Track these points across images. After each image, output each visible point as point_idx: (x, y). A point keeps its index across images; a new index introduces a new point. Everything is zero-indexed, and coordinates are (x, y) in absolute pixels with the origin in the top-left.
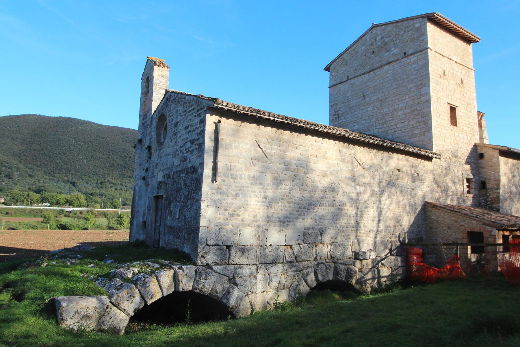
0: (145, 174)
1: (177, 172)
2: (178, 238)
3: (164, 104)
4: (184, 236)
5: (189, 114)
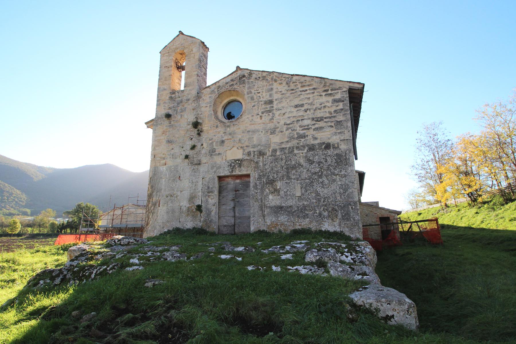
0: (187, 153)
1: (282, 149)
3: (232, 80)
5: (303, 93)
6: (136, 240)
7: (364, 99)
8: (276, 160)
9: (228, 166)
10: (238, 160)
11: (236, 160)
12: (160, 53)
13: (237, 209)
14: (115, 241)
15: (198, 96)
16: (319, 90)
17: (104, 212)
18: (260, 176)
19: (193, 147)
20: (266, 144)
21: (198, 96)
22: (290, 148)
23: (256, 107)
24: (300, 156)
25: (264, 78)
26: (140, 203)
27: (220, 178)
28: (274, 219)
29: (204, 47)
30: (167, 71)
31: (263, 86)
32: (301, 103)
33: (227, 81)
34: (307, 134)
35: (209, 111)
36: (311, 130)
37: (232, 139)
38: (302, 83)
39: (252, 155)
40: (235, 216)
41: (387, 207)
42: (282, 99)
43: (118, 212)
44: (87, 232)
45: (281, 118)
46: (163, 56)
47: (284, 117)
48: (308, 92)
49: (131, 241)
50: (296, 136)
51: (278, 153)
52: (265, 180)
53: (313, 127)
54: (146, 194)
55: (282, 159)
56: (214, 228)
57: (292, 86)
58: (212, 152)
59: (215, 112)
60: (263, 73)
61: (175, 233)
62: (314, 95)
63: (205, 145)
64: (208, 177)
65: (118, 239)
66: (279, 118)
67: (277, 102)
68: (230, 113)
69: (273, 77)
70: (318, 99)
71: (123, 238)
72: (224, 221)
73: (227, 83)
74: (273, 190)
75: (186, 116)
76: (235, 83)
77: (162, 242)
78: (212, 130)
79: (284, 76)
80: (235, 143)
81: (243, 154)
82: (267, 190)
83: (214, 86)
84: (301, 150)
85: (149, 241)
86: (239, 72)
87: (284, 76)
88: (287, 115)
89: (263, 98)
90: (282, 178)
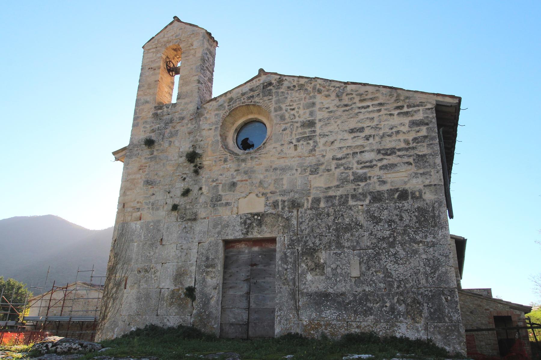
1: (329, 199)
2: (368, 312)
3: (252, 90)
4: (392, 309)
5: (363, 110)
6: (81, 345)
7: (460, 122)
8: (319, 215)
9: (241, 223)
10: (258, 214)
11: (253, 215)
12: (143, 47)
13: (253, 296)
14: (47, 346)
15: (198, 114)
16: (388, 107)
17: (35, 294)
18: (293, 241)
19: (186, 193)
20: (303, 190)
21: (198, 114)
22: (341, 197)
23: (288, 131)
24: (359, 210)
25: (301, 86)
26: (96, 281)
27: (228, 243)
28: (314, 315)
29: (211, 40)
30: (153, 75)
31: (300, 100)
32: (360, 125)
33: (244, 91)
34: (369, 175)
35: (215, 136)
36: (377, 169)
37: (249, 181)
38: (361, 95)
39: (280, 207)
40: (248, 308)
41: (505, 299)
42: (329, 119)
43: (59, 295)
44: (5, 327)
45: (328, 149)
46: (148, 53)
47: (332, 147)
48: (371, 109)
49: (74, 346)
50: (352, 178)
51: (322, 205)
52: (300, 249)
53: (380, 164)
54: (106, 267)
55: (328, 215)
56: (214, 326)
57: (346, 100)
58: (216, 201)
59: (224, 137)
60: (300, 79)
61: (148, 335)
62: (381, 113)
63: (205, 190)
64: (208, 240)
65: (52, 342)
66: (324, 148)
67: (322, 123)
68: (247, 139)
69: (315, 85)
70: (386, 120)
71: (61, 341)
72: (231, 315)
73: (243, 94)
74: (313, 266)
75: (177, 144)
76: (256, 93)
77: (126, 349)
78: (218, 167)
79: (333, 84)
80: (254, 187)
81: (266, 205)
82: (303, 265)
83: (223, 98)
84: (360, 200)
85: (103, 347)
86: (263, 78)
87: (333, 84)
88: (337, 145)
89: (299, 117)
90: (328, 247)
